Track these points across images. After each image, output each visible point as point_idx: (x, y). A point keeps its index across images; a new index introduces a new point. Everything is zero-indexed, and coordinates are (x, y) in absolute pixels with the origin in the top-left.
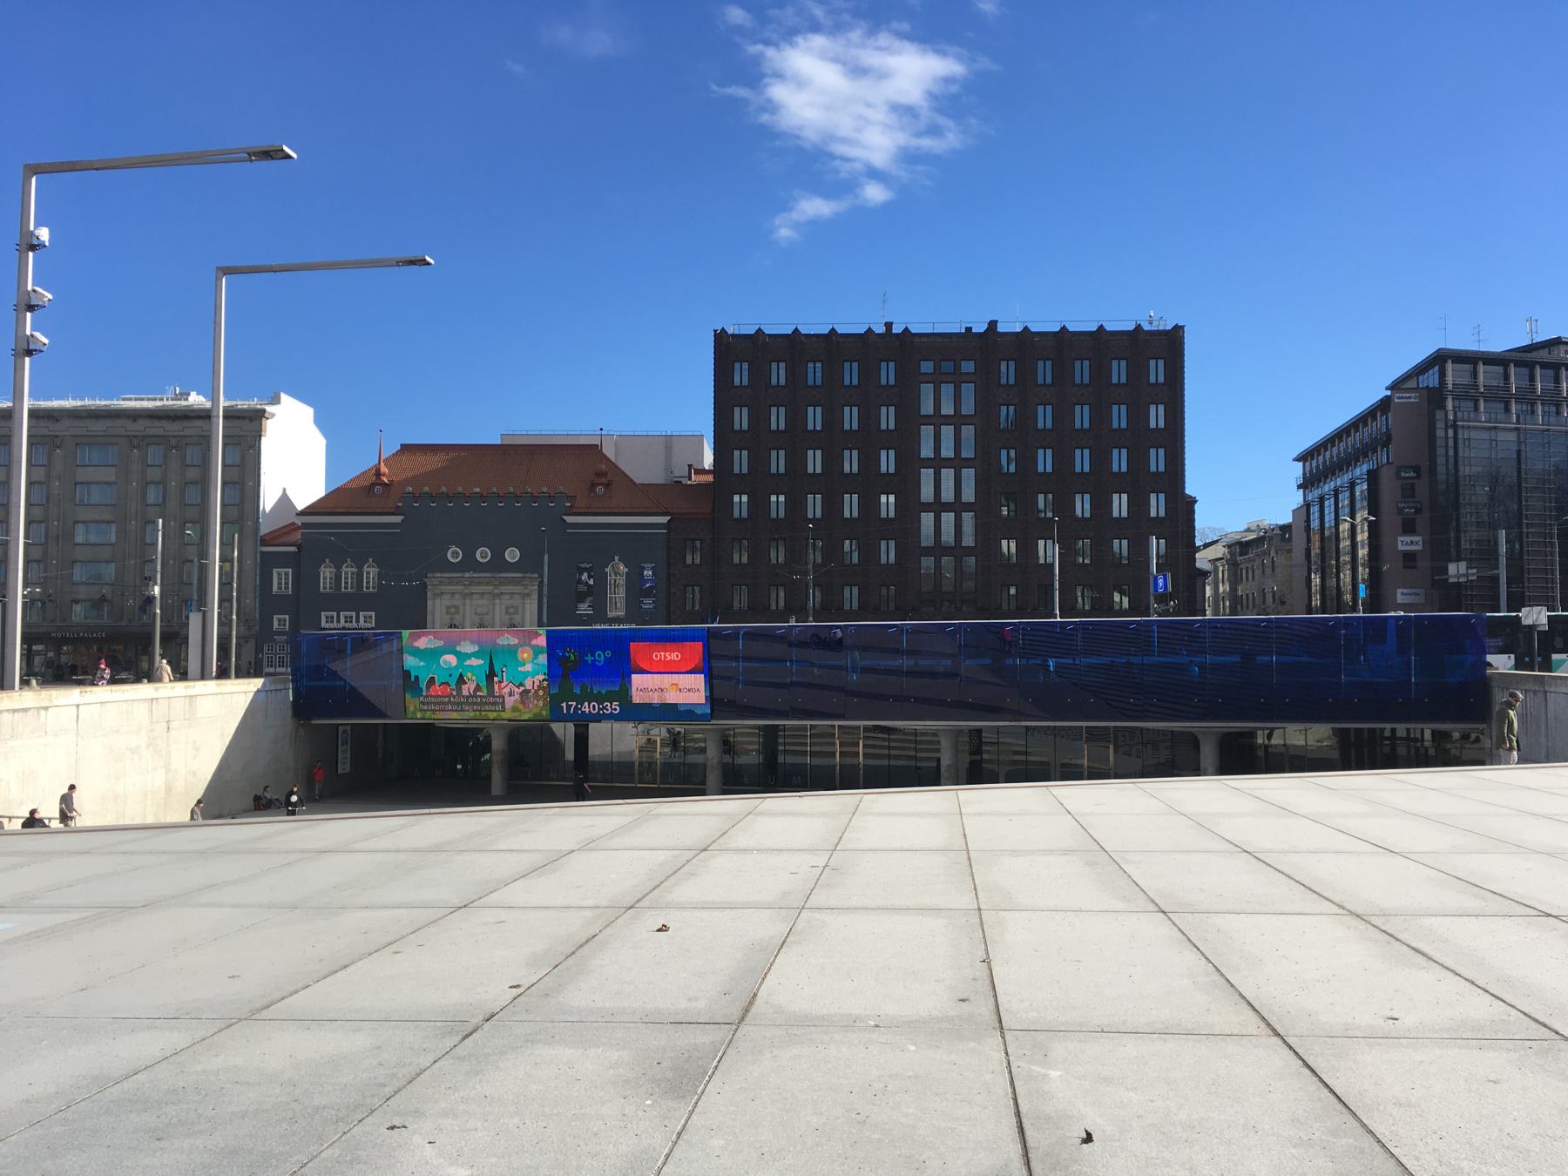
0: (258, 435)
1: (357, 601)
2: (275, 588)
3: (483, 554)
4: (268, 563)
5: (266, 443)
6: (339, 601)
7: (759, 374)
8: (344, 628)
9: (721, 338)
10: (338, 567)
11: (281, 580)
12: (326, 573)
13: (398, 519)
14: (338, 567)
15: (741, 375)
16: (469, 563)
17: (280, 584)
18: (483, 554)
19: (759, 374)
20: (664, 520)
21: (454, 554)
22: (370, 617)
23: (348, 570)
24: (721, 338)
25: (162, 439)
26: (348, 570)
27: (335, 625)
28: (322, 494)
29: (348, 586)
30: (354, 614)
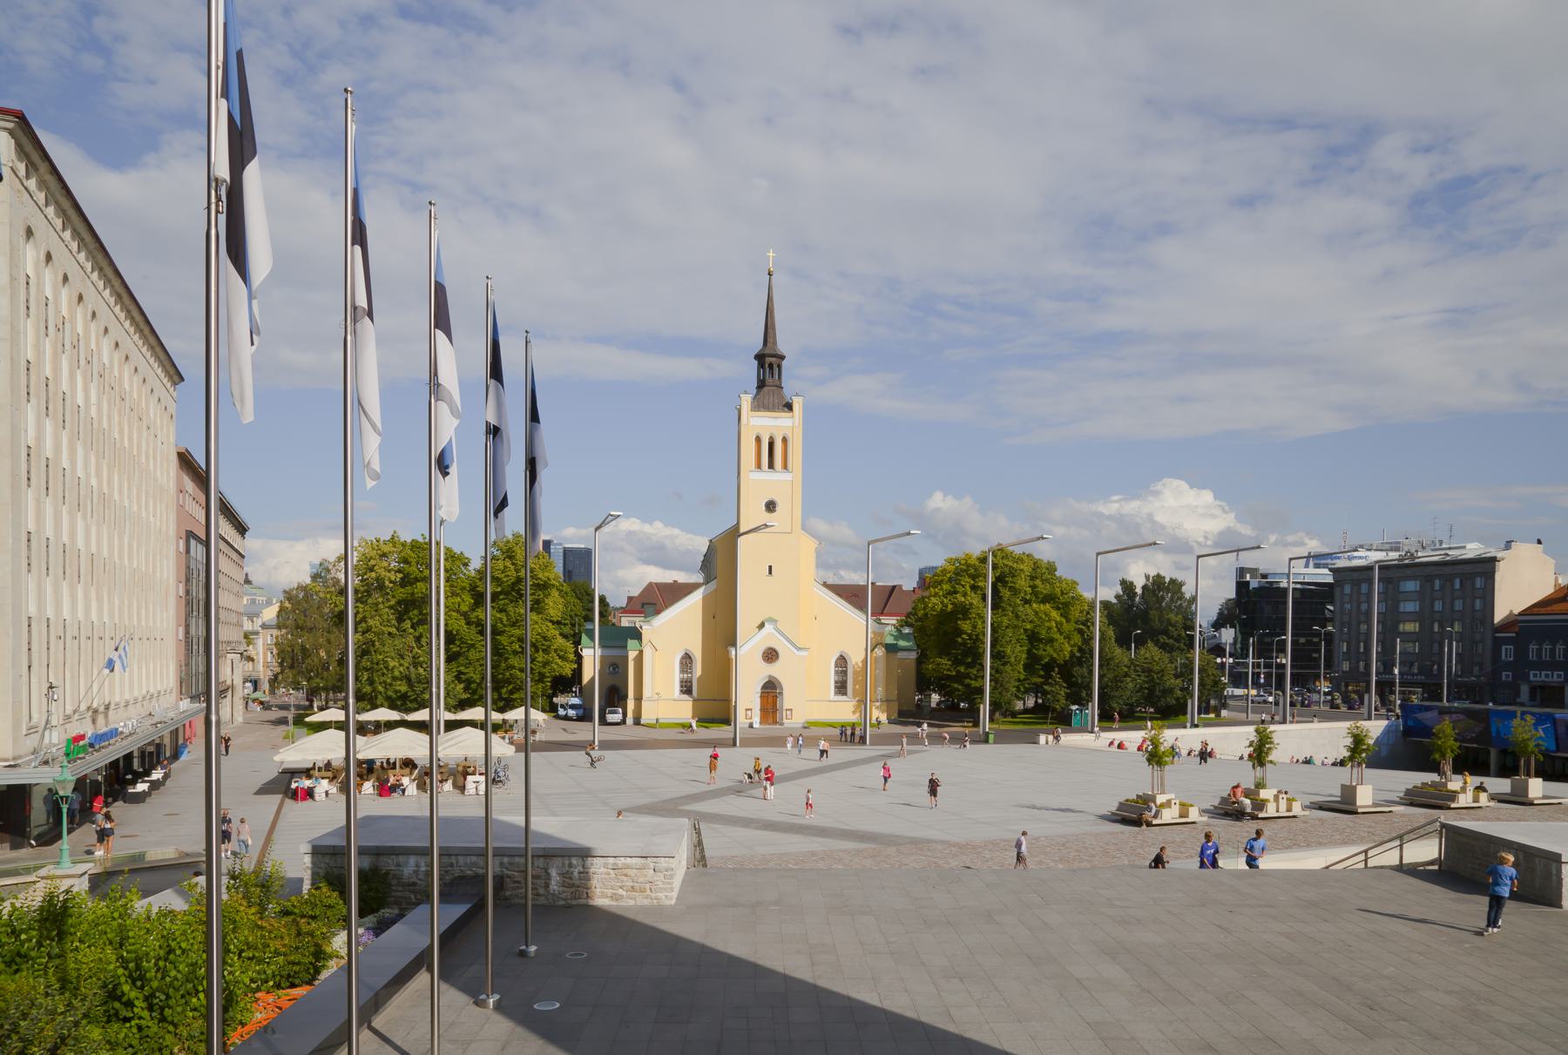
0: (1493, 573)
1: (1552, 666)
4: (1498, 643)
5: (1498, 576)
6: (1540, 665)
8: (1543, 681)
10: (1540, 645)
12: (1533, 647)
14: (1540, 645)
17: (1506, 654)
22: (1558, 675)
23: (1547, 647)
25: (1439, 576)
26: (1547, 647)
27: (1538, 679)
28: (1552, 591)
29: (1546, 657)
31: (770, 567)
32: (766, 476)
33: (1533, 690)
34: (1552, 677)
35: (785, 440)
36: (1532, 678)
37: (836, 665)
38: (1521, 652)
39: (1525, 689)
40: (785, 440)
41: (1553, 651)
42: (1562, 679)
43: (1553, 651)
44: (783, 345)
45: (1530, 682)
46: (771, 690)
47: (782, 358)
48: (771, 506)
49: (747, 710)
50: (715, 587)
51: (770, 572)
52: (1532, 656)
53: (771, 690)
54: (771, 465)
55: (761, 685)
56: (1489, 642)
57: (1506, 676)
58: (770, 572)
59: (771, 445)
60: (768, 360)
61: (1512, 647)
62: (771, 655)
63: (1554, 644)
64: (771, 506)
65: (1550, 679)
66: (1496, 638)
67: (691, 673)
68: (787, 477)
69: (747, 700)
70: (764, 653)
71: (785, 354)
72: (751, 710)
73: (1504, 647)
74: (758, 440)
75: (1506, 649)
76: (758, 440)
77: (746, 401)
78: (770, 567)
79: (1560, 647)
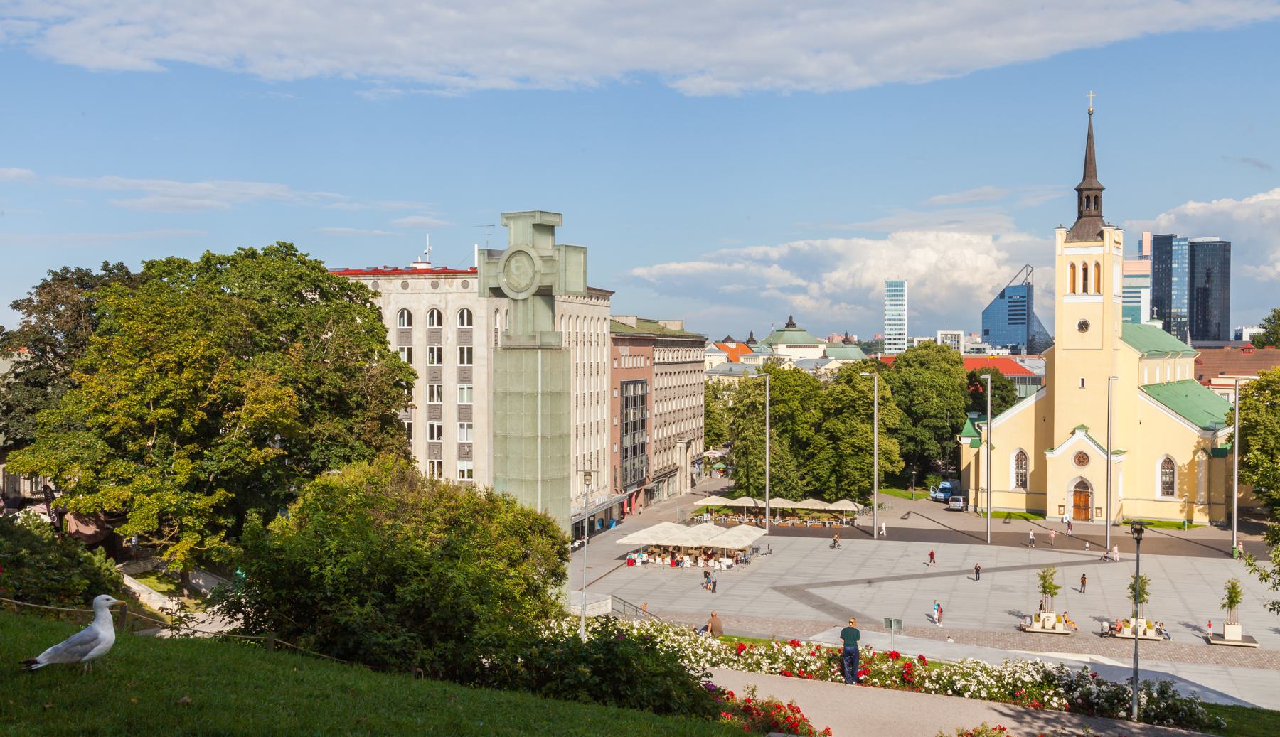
31: (1083, 380)
32: (1081, 299)
35: (1097, 265)
37: (1163, 467)
40: (1097, 265)
44: (1102, 178)
46: (1083, 488)
47: (1102, 189)
48: (1083, 326)
49: (1060, 506)
50: (1045, 394)
51: (1083, 385)
53: (1083, 488)
54: (1085, 289)
55: (1075, 484)
58: (1083, 385)
59: (1085, 271)
60: (1085, 193)
62: (1082, 459)
64: (1083, 326)
67: (1026, 469)
68: (1099, 299)
69: (1059, 499)
70: (1076, 456)
71: (1103, 185)
72: (1063, 506)
74: (1073, 266)
76: (1073, 266)
77: (1061, 235)
78: (1083, 380)
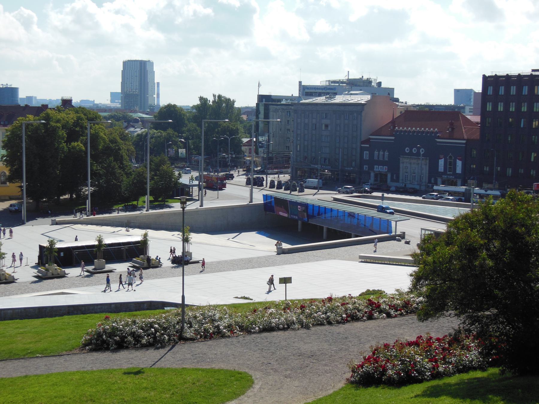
2: (365, 157)
3: (414, 150)
4: (362, 149)
7: (496, 91)
9: (484, 76)
10: (379, 151)
11: (366, 154)
12: (376, 153)
13: (393, 138)
15: (490, 91)
16: (411, 154)
18: (414, 150)
19: (496, 91)
20: (464, 142)
21: (407, 150)
23: (381, 153)
24: (484, 76)
27: (378, 170)
29: (381, 158)
30: (382, 167)
33: (376, 175)
34: (383, 169)
36: (375, 170)
38: (371, 155)
39: (372, 174)
41: (384, 155)
42: (387, 171)
43: (384, 155)
45: (374, 172)
52: (376, 158)
56: (359, 149)
57: (366, 167)
61: (368, 152)
63: (384, 152)
65: (382, 170)
66: (361, 147)
73: (365, 152)
75: (366, 153)
79: (387, 153)
